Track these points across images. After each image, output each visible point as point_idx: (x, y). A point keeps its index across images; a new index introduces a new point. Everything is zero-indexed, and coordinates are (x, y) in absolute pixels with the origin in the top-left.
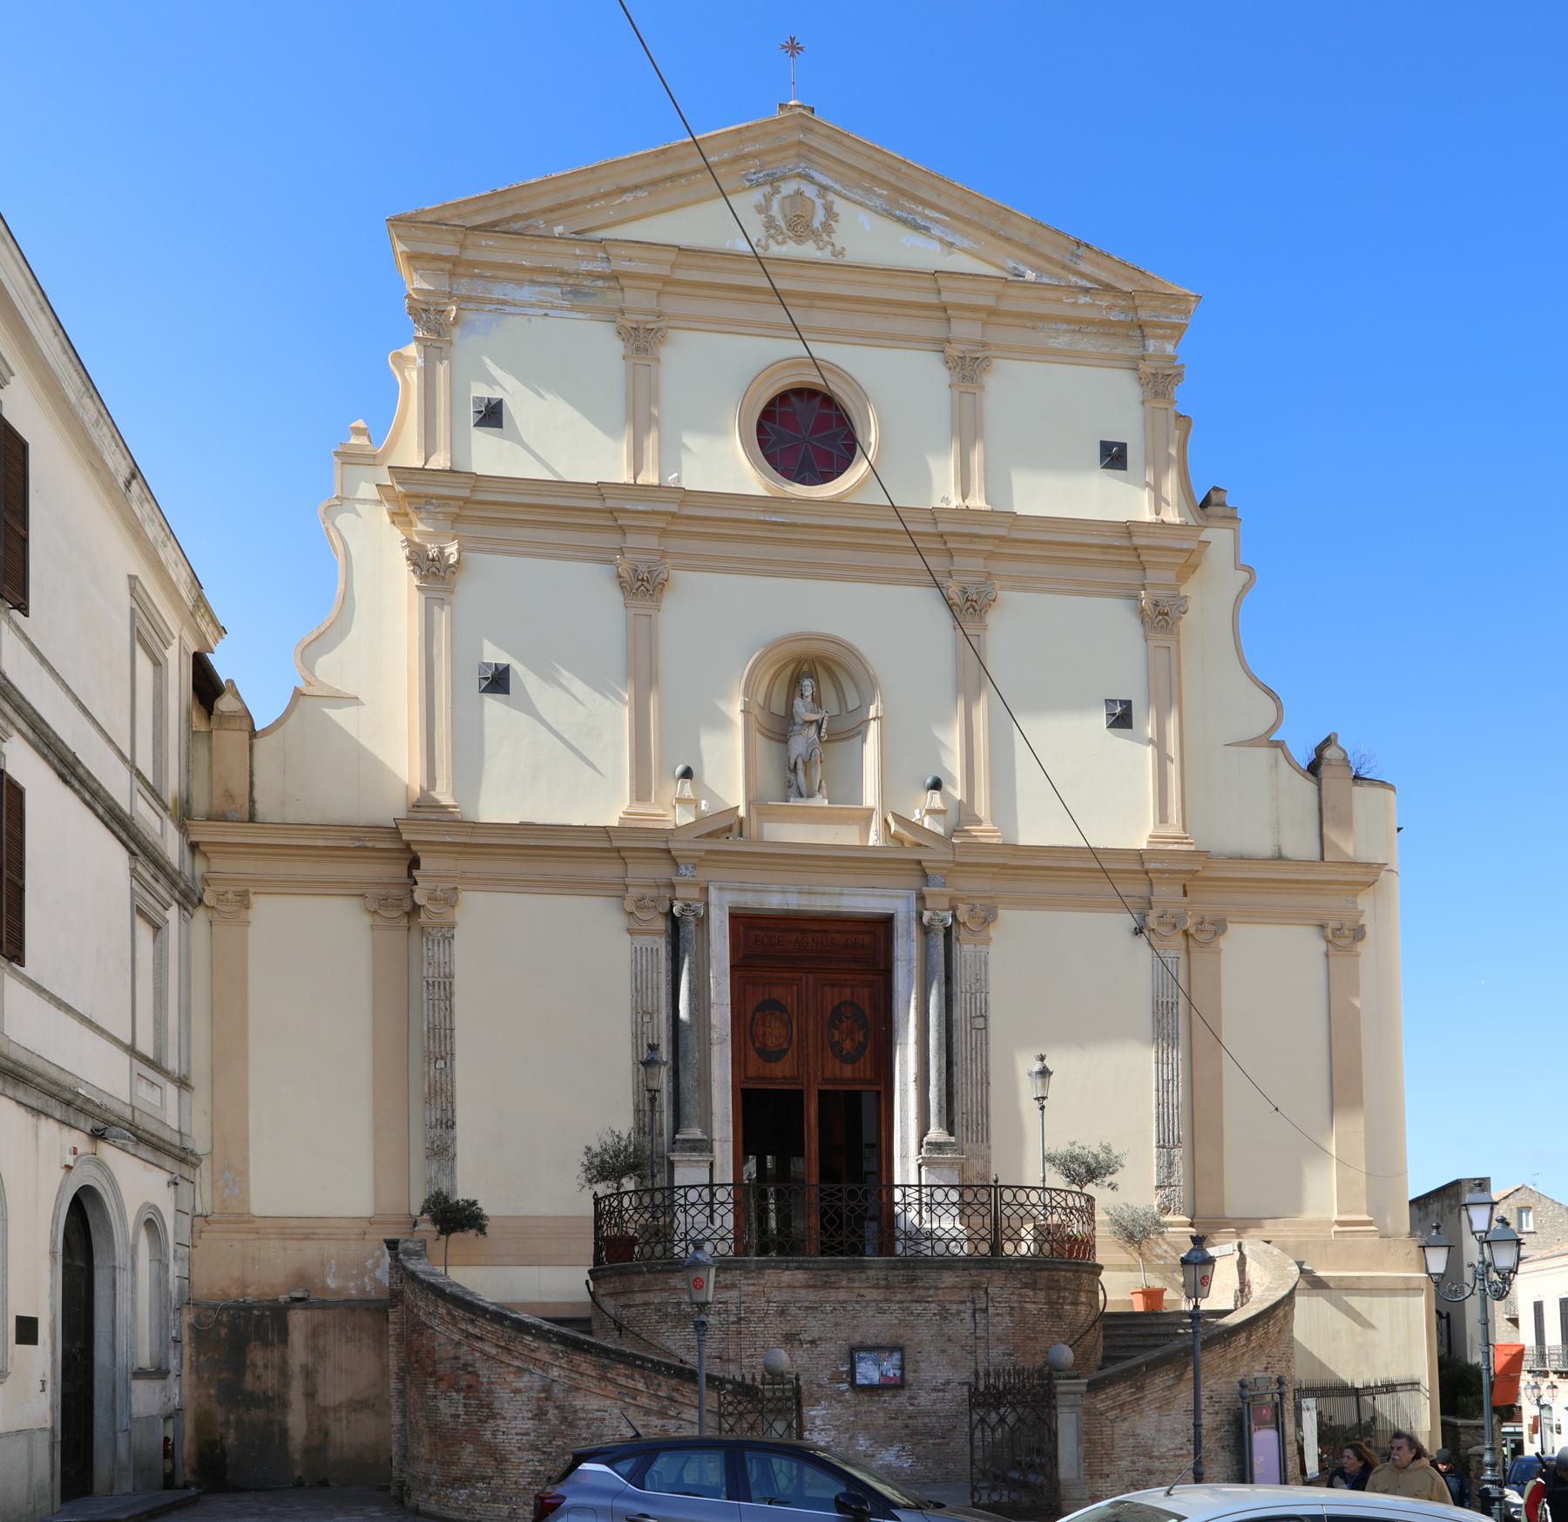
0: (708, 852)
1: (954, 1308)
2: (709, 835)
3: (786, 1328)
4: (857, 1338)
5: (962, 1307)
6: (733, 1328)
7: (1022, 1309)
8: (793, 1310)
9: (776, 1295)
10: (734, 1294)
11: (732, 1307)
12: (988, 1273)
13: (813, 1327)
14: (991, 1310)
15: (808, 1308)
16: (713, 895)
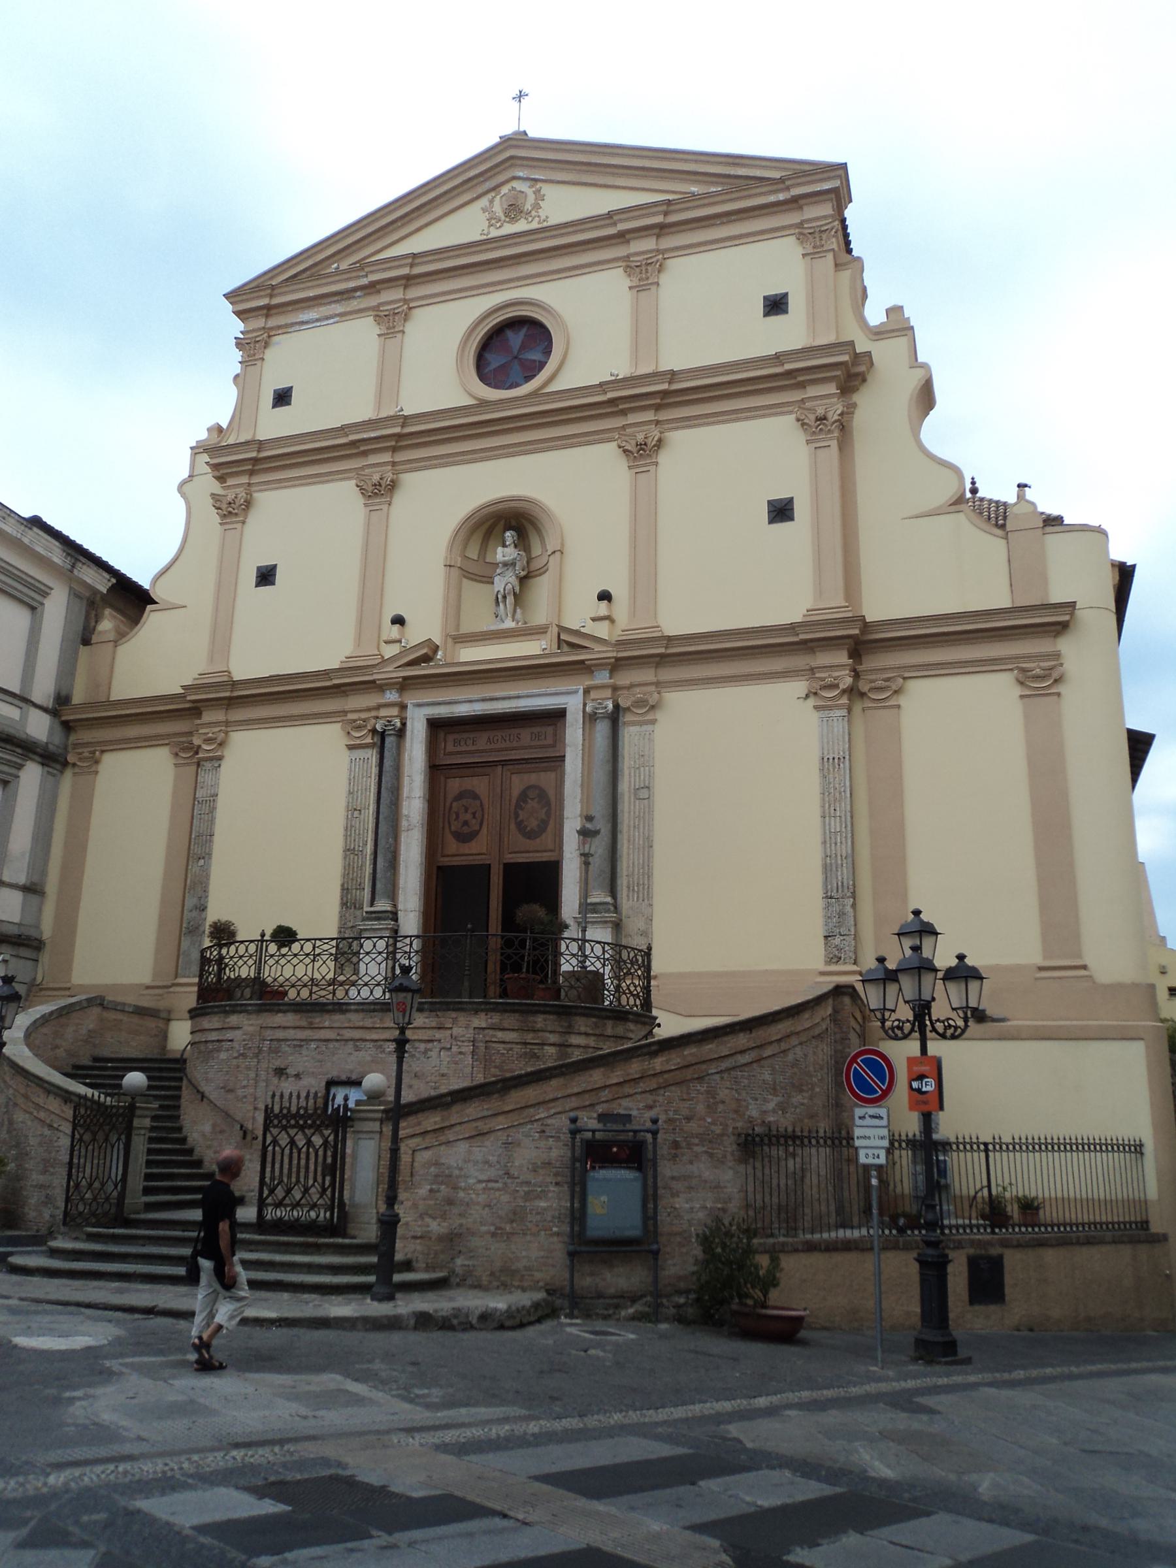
0: (405, 678)
1: (422, 1046)
2: (410, 664)
3: (278, 1063)
4: (334, 1074)
5: (430, 1045)
6: (235, 1062)
7: (486, 1048)
8: (285, 1048)
9: (269, 1034)
10: (238, 1033)
11: (235, 1044)
12: (454, 1014)
13: (299, 1061)
14: (454, 1049)
15: (295, 1046)
16: (411, 712)
